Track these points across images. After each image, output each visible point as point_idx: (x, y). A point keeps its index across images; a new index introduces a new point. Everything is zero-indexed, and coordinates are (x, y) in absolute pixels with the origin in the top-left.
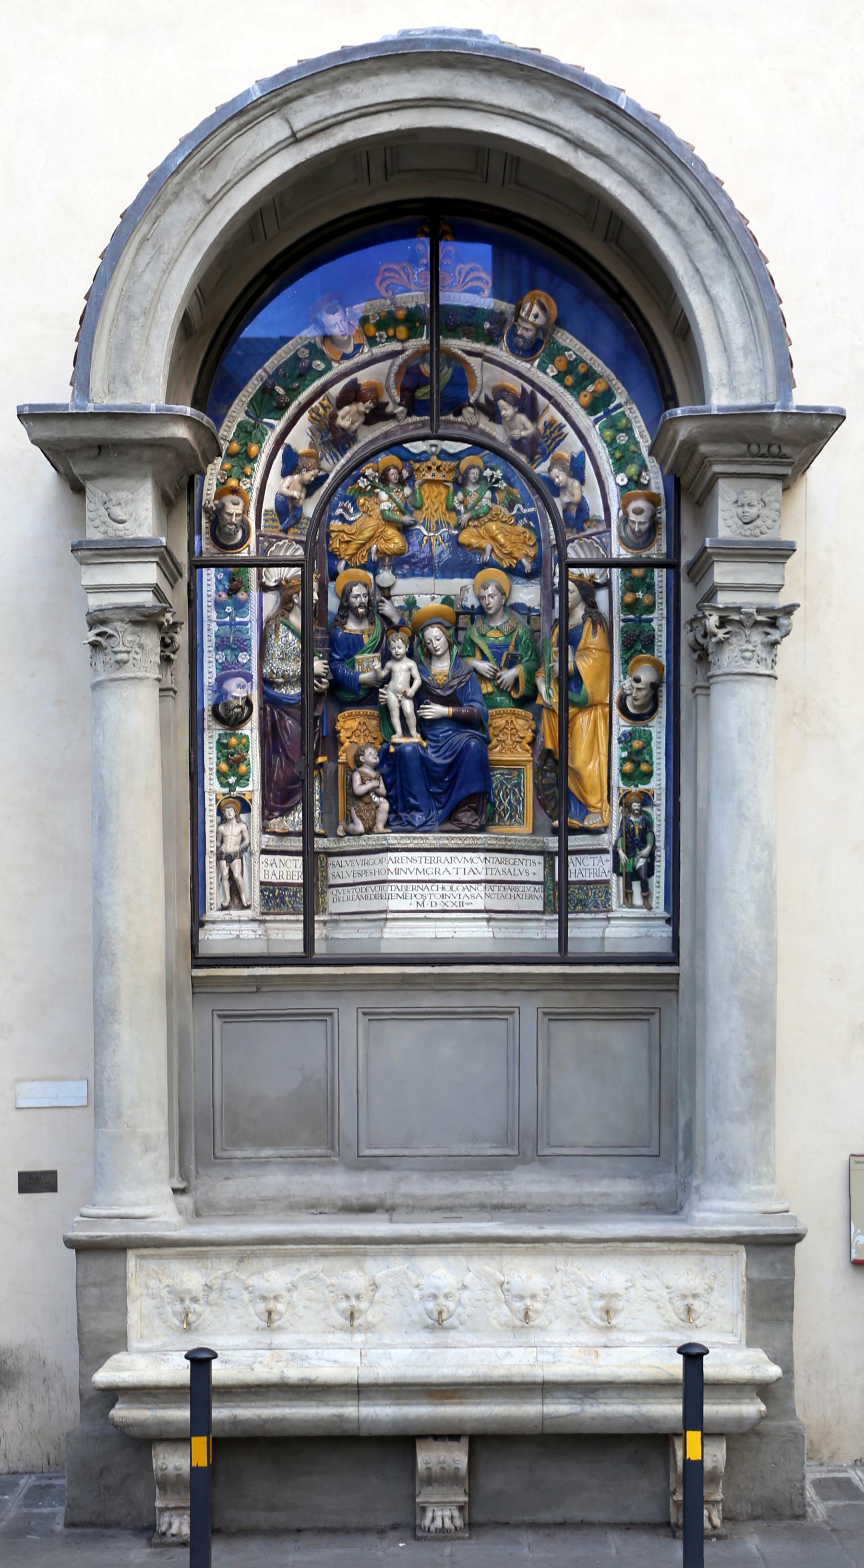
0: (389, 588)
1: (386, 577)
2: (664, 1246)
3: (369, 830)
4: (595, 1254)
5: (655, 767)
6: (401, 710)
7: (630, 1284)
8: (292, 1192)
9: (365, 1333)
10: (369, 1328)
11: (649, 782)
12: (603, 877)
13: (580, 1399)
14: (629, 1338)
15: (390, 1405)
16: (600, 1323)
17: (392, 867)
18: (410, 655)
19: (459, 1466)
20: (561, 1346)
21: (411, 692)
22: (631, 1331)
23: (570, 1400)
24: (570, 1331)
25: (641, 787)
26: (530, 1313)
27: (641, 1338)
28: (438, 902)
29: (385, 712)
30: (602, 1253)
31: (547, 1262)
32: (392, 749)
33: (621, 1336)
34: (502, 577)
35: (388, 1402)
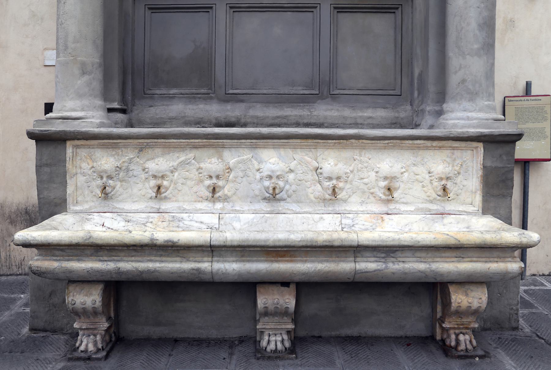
2: (429, 143)
4: (380, 149)
7: (404, 170)
8: (187, 114)
9: (224, 202)
10: (226, 199)
13: (383, 258)
14: (403, 208)
15: (236, 261)
16: (383, 197)
19: (289, 306)
20: (357, 213)
22: (403, 203)
23: (376, 259)
24: (362, 203)
26: (336, 190)
27: (412, 208)
30: (385, 148)
31: (347, 154)
33: (398, 206)
35: (234, 259)
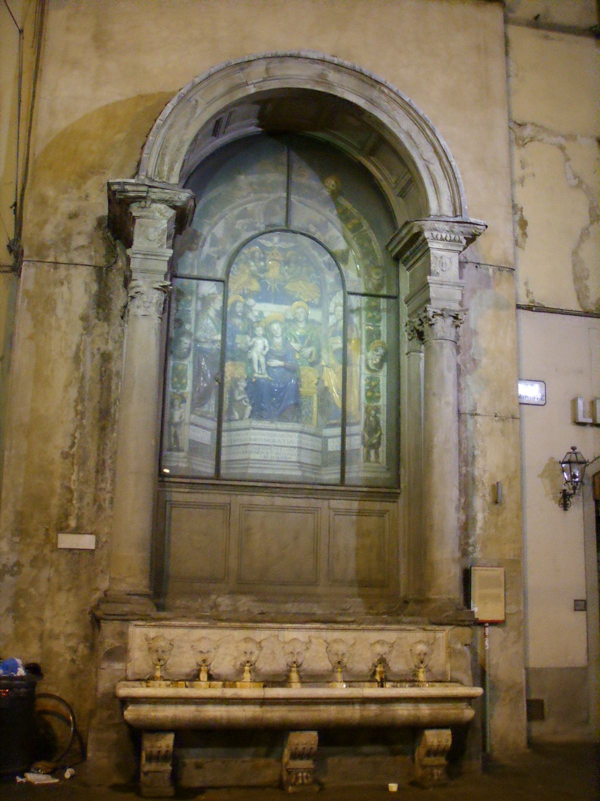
0: (252, 306)
1: (251, 302)
3: (241, 418)
5: (381, 394)
6: (259, 361)
11: (378, 401)
12: (356, 447)
17: (253, 437)
18: (264, 336)
21: (265, 353)
25: (375, 404)
28: (275, 456)
29: (251, 361)
32: (254, 380)
34: (305, 305)
